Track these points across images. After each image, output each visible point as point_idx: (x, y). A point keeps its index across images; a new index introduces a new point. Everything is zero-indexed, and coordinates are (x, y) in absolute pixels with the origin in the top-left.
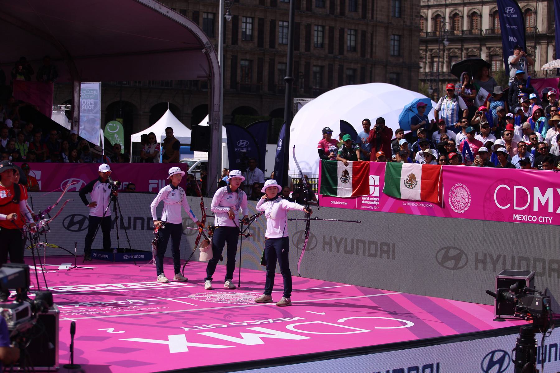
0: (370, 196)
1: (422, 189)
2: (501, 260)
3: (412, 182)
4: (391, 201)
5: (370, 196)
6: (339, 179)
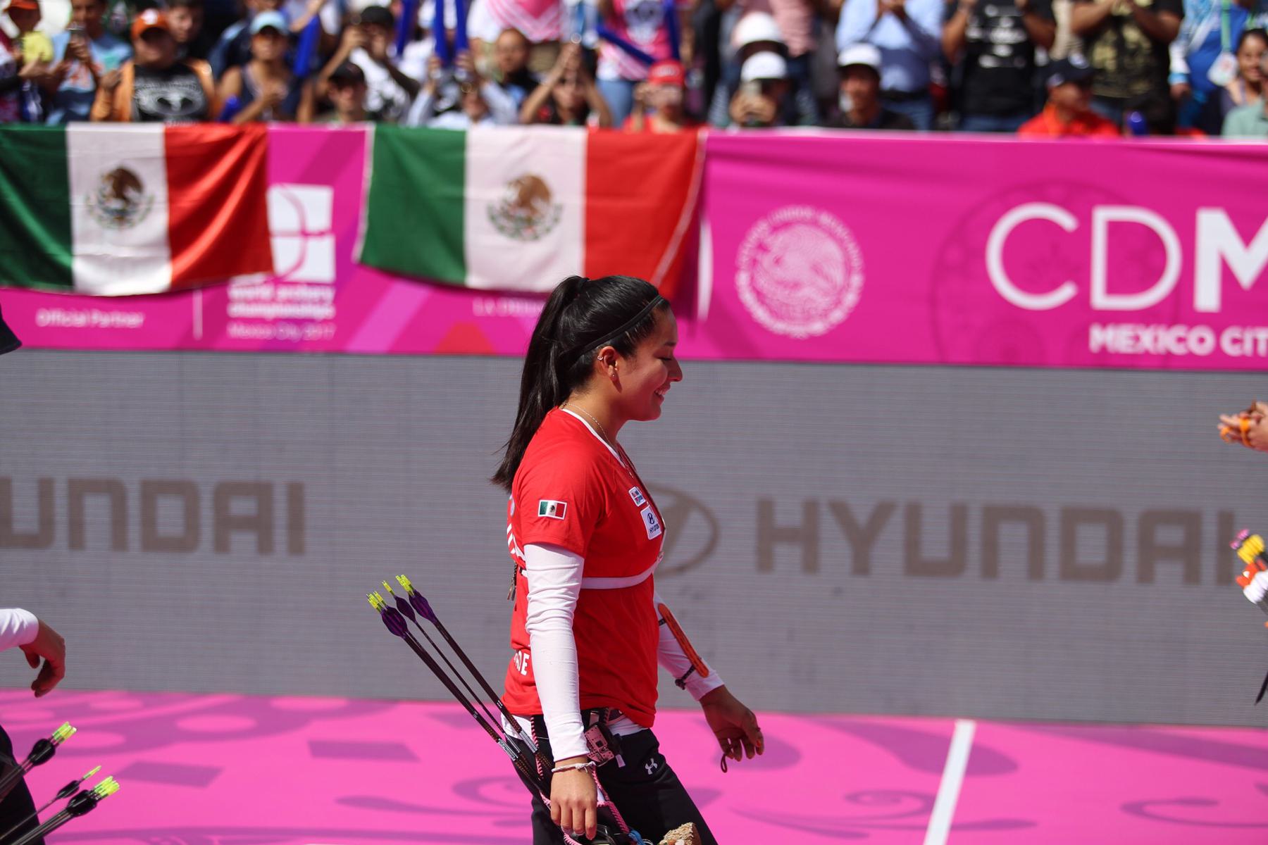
0: (278, 281)
1: (592, 238)
3: (533, 210)
4: (404, 300)
5: (278, 281)
6: (80, 203)
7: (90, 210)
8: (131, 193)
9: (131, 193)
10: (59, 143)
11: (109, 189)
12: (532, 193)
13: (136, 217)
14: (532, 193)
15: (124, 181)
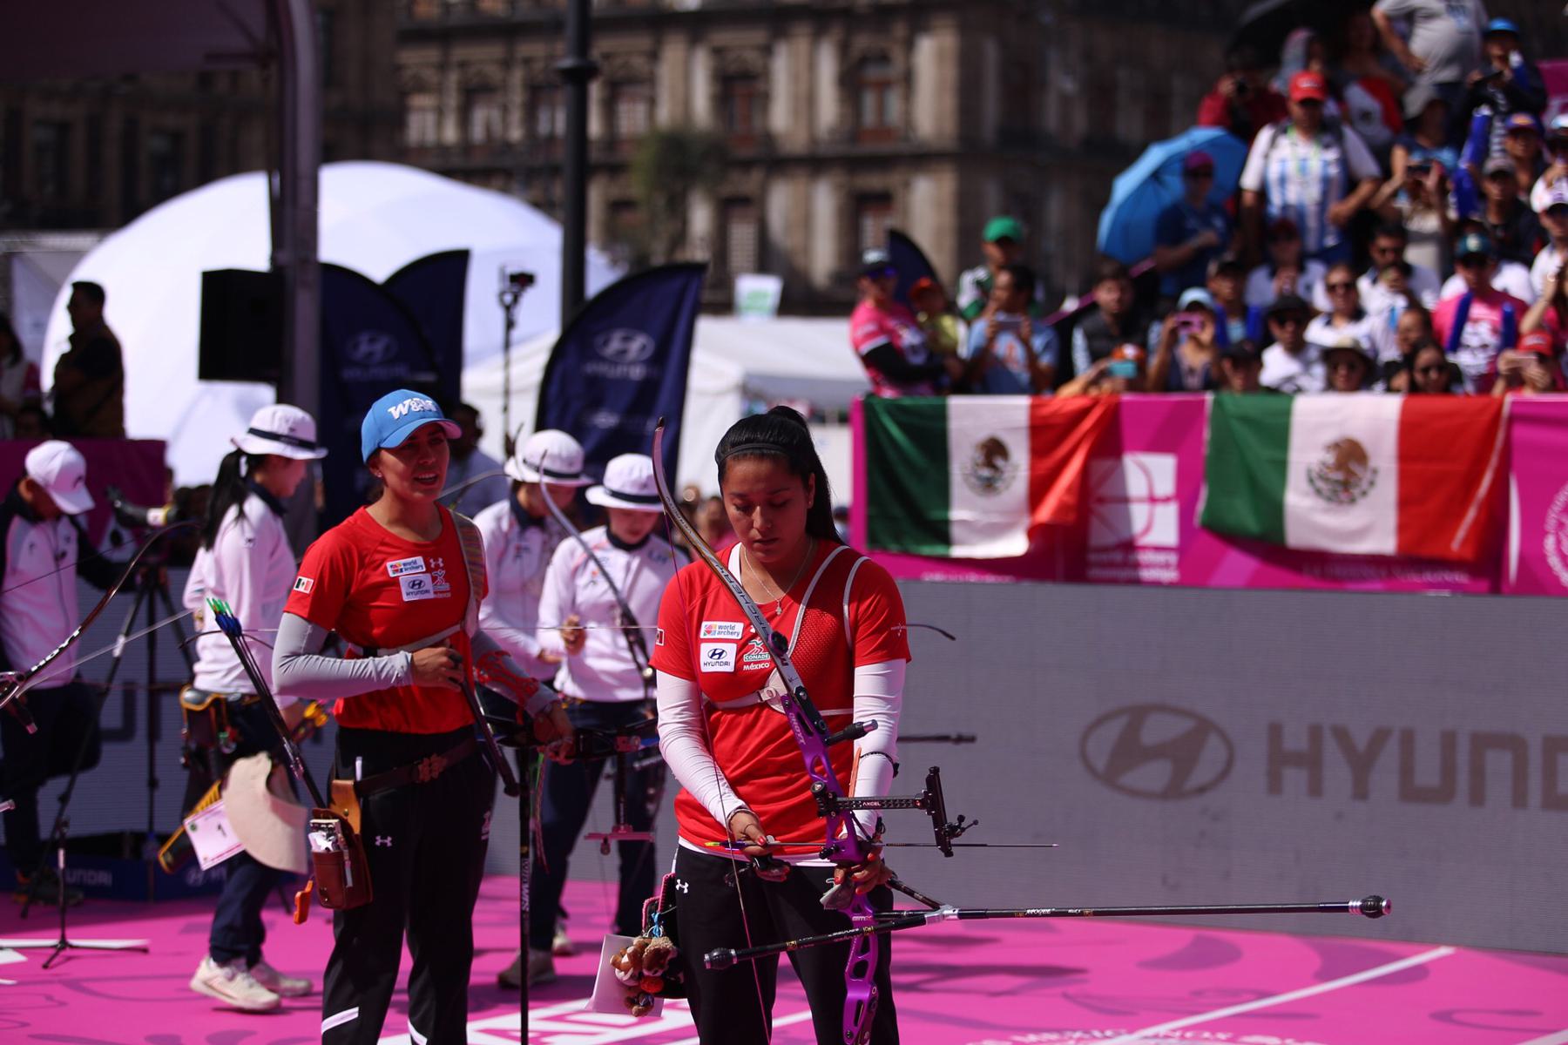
1: (1405, 503)
2: (1390, 754)
3: (1350, 473)
7: (966, 478)
8: (999, 462)
9: (999, 462)
10: (941, 415)
11: (981, 460)
12: (1350, 455)
13: (999, 484)
14: (1350, 455)
15: (994, 450)
